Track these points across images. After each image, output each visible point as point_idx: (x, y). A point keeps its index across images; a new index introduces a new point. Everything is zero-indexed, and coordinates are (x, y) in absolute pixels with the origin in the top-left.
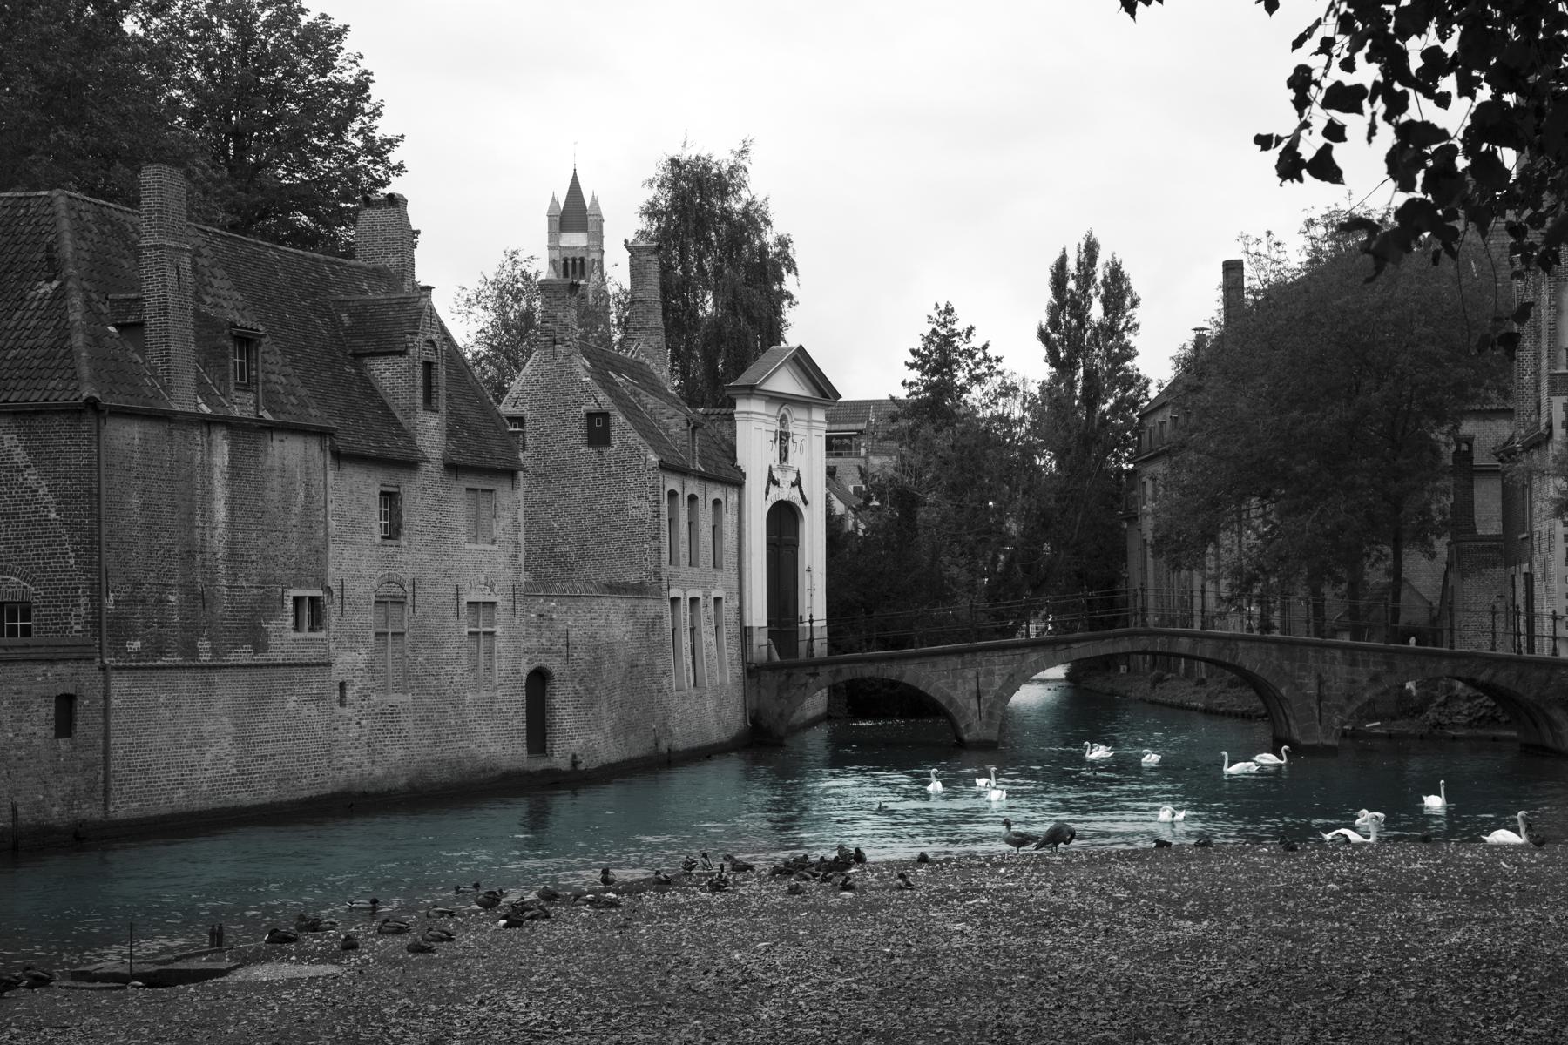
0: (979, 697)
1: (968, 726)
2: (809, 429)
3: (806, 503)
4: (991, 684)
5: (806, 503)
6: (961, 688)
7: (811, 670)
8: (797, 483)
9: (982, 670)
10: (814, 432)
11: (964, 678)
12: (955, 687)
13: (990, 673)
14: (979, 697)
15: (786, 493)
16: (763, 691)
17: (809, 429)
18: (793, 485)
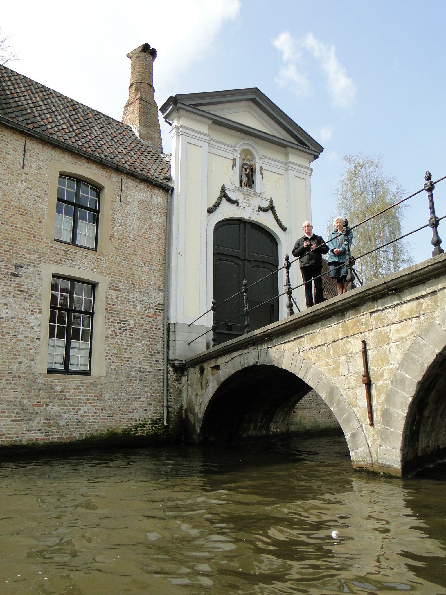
0: (369, 385)
1: (354, 435)
2: (287, 170)
3: (284, 229)
4: (385, 360)
5: (284, 229)
6: (344, 371)
7: (213, 363)
8: (272, 208)
9: (370, 337)
10: (292, 173)
11: (348, 355)
12: (336, 370)
13: (385, 339)
14: (369, 385)
15: (248, 211)
16: (190, 388)
17: (287, 170)
18: (261, 209)
